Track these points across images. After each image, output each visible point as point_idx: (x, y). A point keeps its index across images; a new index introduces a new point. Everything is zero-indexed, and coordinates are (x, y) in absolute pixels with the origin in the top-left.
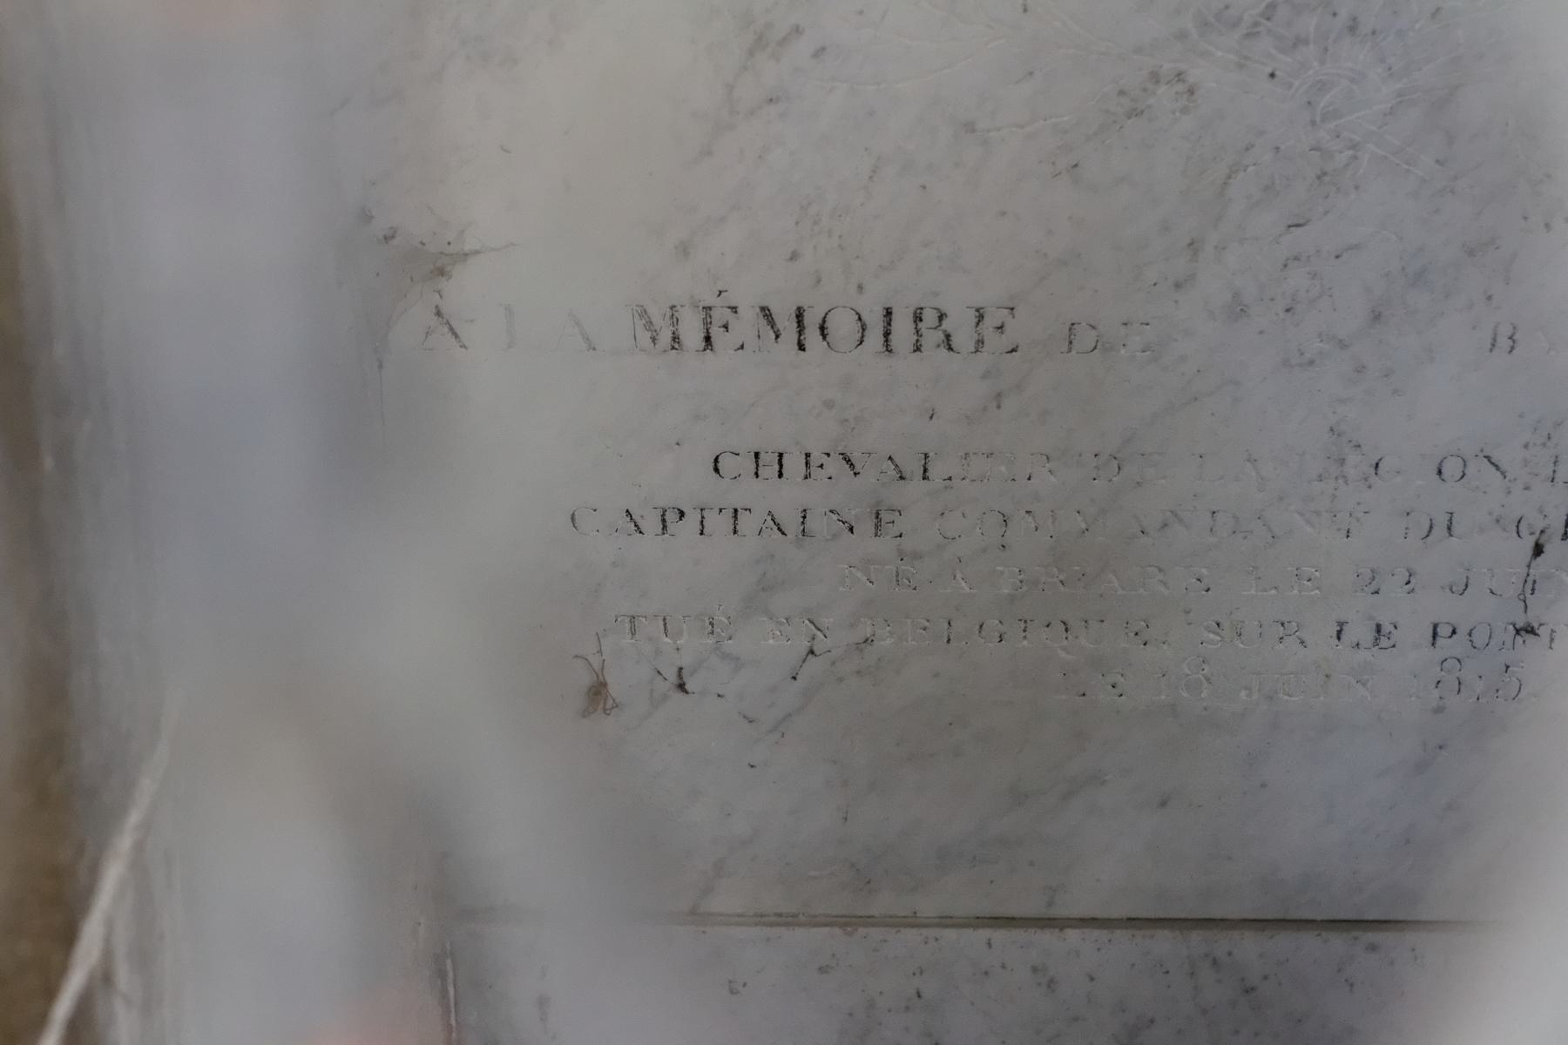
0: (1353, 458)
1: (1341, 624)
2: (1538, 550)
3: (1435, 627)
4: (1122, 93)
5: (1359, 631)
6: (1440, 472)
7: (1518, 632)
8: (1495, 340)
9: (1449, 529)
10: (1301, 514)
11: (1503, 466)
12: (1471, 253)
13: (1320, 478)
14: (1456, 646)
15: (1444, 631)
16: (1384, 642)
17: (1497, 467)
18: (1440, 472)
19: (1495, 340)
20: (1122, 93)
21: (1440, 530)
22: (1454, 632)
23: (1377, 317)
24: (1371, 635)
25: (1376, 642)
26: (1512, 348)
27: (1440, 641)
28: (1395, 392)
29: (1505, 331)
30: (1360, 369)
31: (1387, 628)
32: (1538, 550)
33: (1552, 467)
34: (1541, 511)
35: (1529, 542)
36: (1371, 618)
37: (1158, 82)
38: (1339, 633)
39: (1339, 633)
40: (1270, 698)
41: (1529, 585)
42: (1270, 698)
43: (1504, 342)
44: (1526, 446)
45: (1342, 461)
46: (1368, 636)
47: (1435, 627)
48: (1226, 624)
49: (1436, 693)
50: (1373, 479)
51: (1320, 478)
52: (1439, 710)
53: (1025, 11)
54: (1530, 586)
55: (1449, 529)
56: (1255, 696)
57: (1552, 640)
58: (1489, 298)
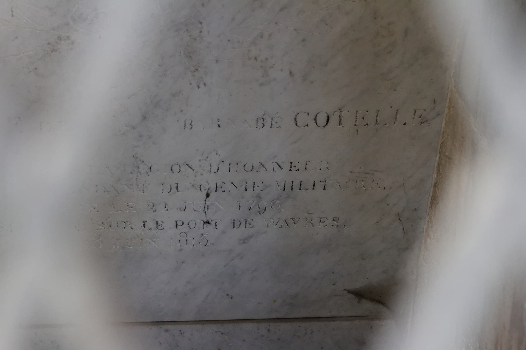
0: (142, 166)
1: (144, 222)
2: (208, 195)
3: (176, 222)
4: (49, 44)
5: (151, 224)
6: (172, 170)
7: (204, 223)
8: (185, 125)
9: (177, 189)
10: (126, 185)
11: (193, 167)
12: (174, 95)
13: (131, 173)
14: (184, 228)
15: (179, 223)
16: (160, 228)
17: (191, 168)
18: (172, 170)
19: (185, 125)
20: (49, 44)
21: (174, 189)
22: (183, 224)
23: (144, 118)
24: (155, 226)
25: (157, 228)
26: (191, 128)
27: (178, 227)
28: (154, 143)
29: (188, 122)
30: (141, 136)
31: (160, 223)
32: (208, 195)
33: (209, 168)
34: (207, 182)
35: (204, 193)
36: (154, 220)
37: (61, 40)
38: (144, 225)
39: (144, 225)
40: (123, 248)
41: (206, 206)
42: (123, 248)
43: (188, 126)
44: (200, 160)
45: (138, 167)
46: (154, 226)
47: (176, 222)
48: (105, 223)
49: (179, 244)
50: (150, 173)
51: (131, 173)
52: (181, 250)
53: (13, 16)
54: (206, 208)
55: (177, 189)
56: (118, 247)
57: (216, 225)
58: (182, 111)
